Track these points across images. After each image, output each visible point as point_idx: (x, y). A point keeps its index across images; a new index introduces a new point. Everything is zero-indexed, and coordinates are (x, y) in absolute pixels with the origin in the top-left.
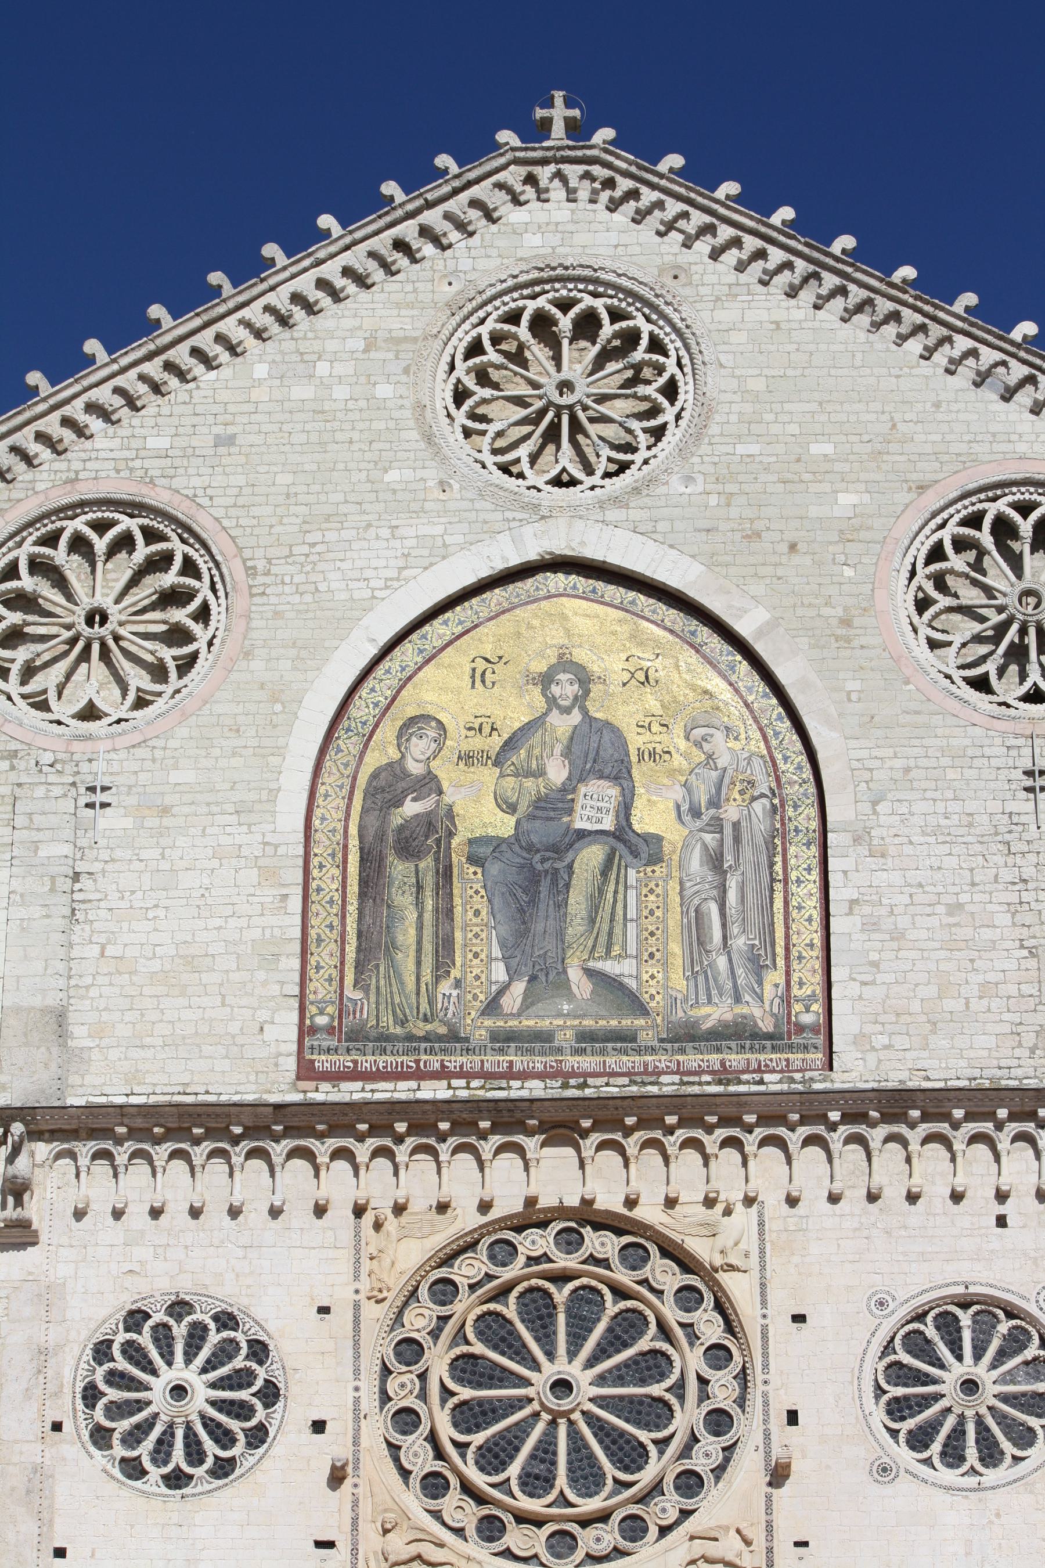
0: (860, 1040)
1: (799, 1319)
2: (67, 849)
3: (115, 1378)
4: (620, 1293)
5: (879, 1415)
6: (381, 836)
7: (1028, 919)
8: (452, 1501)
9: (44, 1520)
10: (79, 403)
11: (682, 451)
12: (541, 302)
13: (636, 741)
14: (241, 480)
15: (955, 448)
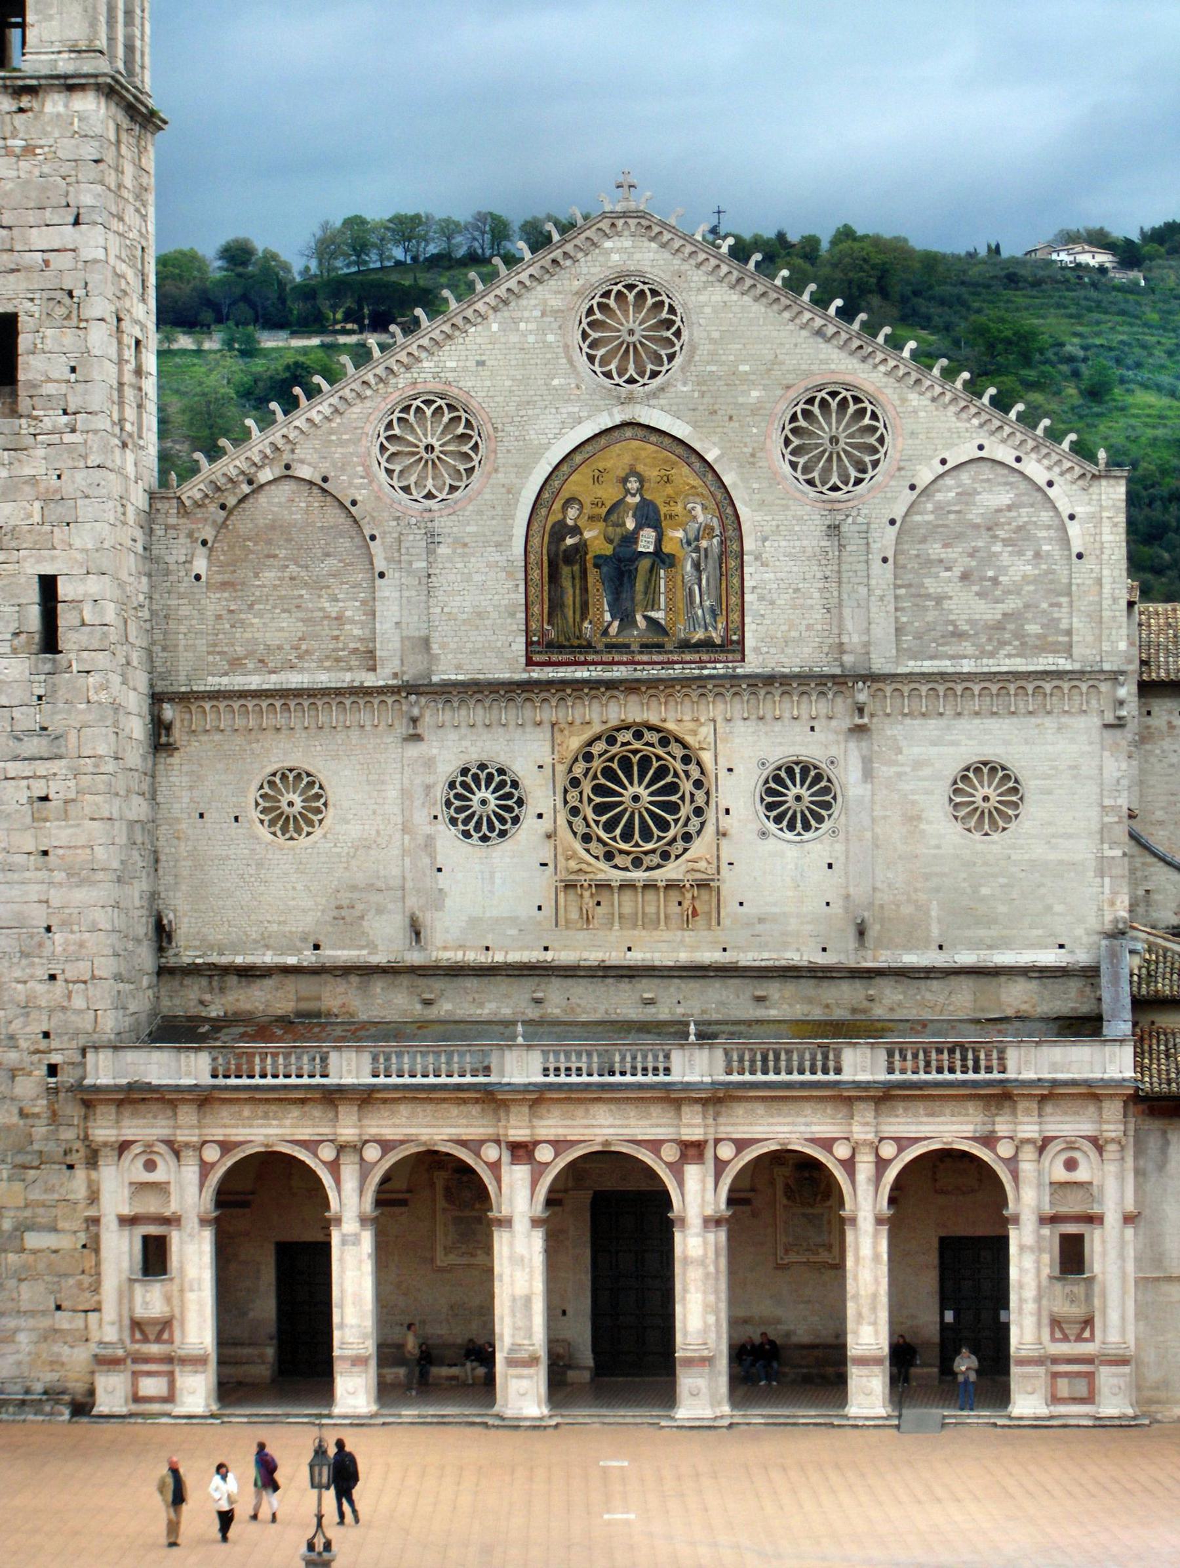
0: (757, 650)
1: (730, 770)
2: (424, 564)
3: (458, 796)
4: (659, 758)
5: (761, 809)
6: (557, 555)
7: (827, 595)
8: (593, 845)
9: (433, 858)
10: (415, 346)
11: (683, 369)
12: (619, 287)
13: (663, 510)
14: (488, 383)
15: (804, 367)
